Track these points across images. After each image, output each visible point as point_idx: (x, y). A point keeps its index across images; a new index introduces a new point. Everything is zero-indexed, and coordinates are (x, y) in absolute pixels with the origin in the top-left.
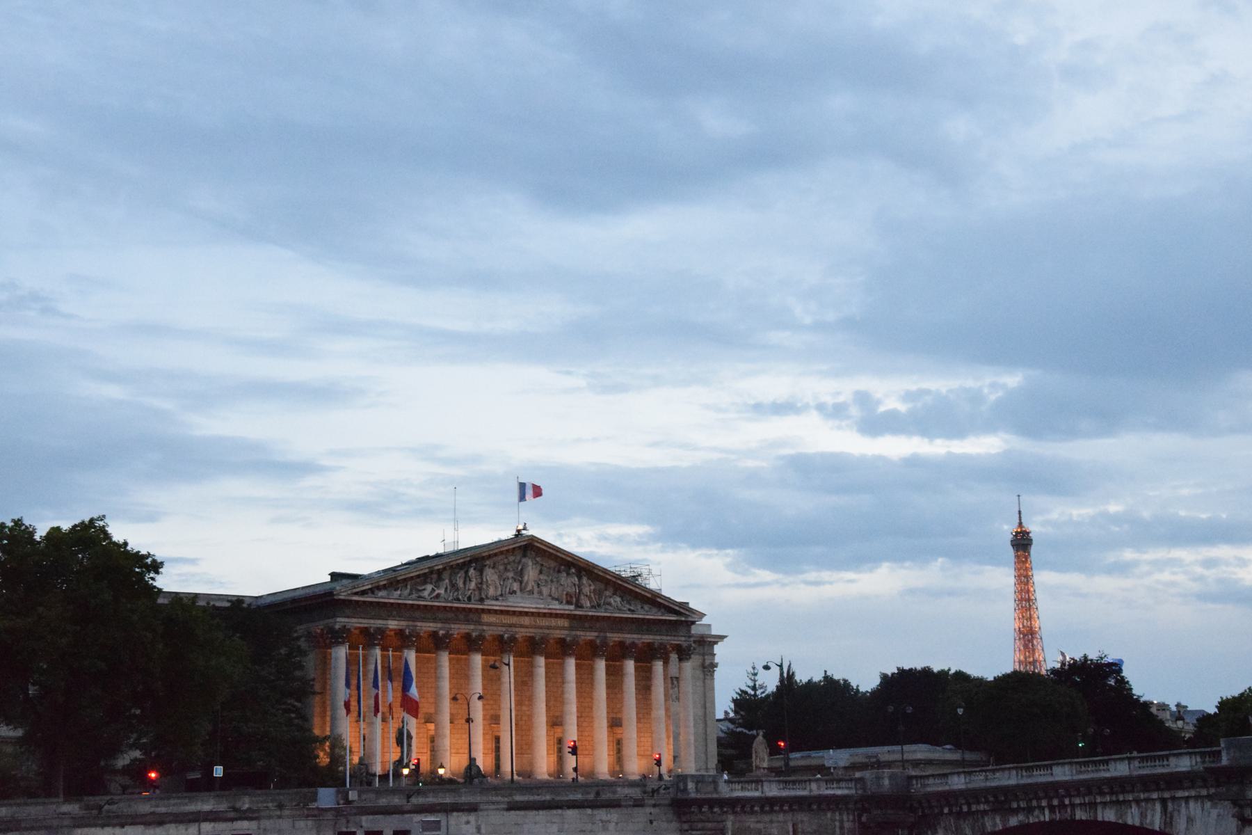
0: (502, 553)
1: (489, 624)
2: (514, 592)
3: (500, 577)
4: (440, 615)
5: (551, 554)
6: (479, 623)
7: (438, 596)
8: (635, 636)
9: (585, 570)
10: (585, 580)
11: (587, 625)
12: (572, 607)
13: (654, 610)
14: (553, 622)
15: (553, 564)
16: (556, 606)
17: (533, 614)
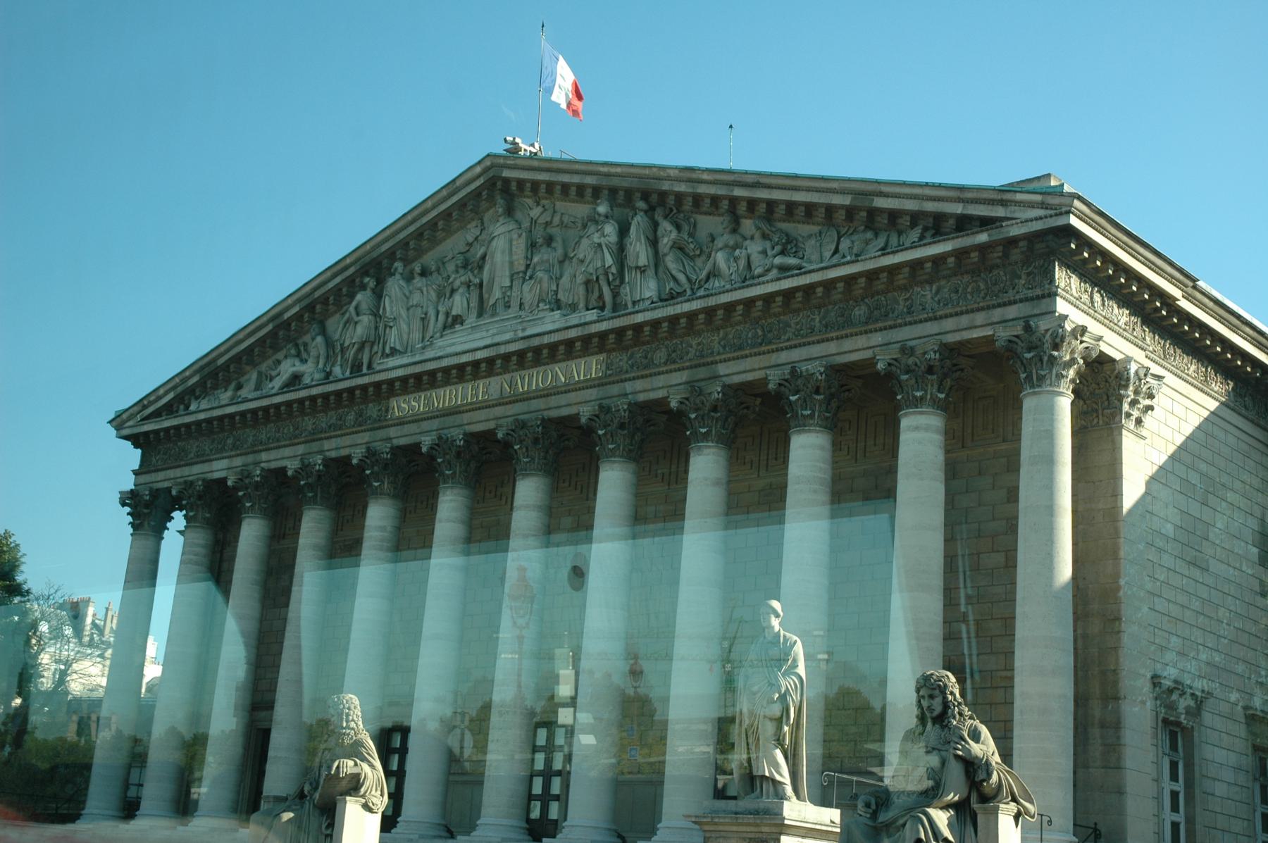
0: (433, 225)
1: (401, 422)
2: (458, 320)
3: (440, 295)
4: (308, 423)
5: (550, 186)
6: (381, 423)
7: (296, 379)
8: (816, 350)
9: (645, 196)
10: (638, 224)
11: (660, 355)
12: (592, 315)
13: (881, 242)
14: (559, 373)
15: (580, 210)
16: (550, 324)
17: (490, 361)
